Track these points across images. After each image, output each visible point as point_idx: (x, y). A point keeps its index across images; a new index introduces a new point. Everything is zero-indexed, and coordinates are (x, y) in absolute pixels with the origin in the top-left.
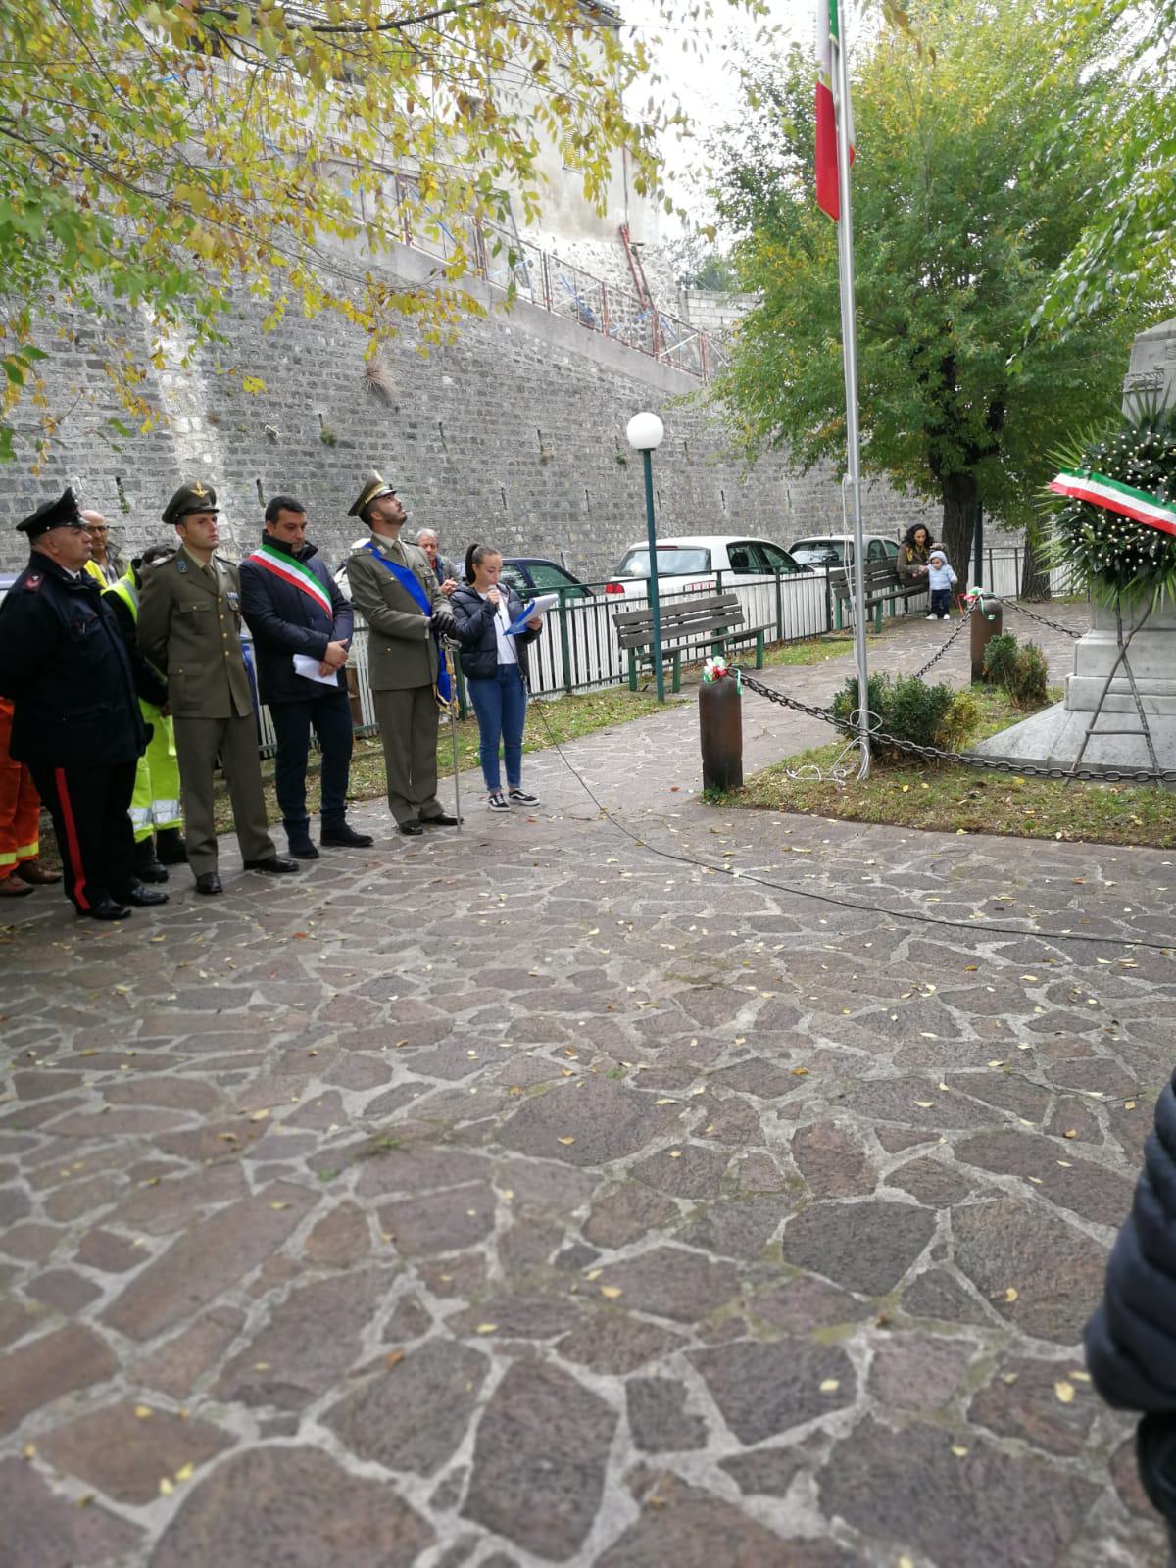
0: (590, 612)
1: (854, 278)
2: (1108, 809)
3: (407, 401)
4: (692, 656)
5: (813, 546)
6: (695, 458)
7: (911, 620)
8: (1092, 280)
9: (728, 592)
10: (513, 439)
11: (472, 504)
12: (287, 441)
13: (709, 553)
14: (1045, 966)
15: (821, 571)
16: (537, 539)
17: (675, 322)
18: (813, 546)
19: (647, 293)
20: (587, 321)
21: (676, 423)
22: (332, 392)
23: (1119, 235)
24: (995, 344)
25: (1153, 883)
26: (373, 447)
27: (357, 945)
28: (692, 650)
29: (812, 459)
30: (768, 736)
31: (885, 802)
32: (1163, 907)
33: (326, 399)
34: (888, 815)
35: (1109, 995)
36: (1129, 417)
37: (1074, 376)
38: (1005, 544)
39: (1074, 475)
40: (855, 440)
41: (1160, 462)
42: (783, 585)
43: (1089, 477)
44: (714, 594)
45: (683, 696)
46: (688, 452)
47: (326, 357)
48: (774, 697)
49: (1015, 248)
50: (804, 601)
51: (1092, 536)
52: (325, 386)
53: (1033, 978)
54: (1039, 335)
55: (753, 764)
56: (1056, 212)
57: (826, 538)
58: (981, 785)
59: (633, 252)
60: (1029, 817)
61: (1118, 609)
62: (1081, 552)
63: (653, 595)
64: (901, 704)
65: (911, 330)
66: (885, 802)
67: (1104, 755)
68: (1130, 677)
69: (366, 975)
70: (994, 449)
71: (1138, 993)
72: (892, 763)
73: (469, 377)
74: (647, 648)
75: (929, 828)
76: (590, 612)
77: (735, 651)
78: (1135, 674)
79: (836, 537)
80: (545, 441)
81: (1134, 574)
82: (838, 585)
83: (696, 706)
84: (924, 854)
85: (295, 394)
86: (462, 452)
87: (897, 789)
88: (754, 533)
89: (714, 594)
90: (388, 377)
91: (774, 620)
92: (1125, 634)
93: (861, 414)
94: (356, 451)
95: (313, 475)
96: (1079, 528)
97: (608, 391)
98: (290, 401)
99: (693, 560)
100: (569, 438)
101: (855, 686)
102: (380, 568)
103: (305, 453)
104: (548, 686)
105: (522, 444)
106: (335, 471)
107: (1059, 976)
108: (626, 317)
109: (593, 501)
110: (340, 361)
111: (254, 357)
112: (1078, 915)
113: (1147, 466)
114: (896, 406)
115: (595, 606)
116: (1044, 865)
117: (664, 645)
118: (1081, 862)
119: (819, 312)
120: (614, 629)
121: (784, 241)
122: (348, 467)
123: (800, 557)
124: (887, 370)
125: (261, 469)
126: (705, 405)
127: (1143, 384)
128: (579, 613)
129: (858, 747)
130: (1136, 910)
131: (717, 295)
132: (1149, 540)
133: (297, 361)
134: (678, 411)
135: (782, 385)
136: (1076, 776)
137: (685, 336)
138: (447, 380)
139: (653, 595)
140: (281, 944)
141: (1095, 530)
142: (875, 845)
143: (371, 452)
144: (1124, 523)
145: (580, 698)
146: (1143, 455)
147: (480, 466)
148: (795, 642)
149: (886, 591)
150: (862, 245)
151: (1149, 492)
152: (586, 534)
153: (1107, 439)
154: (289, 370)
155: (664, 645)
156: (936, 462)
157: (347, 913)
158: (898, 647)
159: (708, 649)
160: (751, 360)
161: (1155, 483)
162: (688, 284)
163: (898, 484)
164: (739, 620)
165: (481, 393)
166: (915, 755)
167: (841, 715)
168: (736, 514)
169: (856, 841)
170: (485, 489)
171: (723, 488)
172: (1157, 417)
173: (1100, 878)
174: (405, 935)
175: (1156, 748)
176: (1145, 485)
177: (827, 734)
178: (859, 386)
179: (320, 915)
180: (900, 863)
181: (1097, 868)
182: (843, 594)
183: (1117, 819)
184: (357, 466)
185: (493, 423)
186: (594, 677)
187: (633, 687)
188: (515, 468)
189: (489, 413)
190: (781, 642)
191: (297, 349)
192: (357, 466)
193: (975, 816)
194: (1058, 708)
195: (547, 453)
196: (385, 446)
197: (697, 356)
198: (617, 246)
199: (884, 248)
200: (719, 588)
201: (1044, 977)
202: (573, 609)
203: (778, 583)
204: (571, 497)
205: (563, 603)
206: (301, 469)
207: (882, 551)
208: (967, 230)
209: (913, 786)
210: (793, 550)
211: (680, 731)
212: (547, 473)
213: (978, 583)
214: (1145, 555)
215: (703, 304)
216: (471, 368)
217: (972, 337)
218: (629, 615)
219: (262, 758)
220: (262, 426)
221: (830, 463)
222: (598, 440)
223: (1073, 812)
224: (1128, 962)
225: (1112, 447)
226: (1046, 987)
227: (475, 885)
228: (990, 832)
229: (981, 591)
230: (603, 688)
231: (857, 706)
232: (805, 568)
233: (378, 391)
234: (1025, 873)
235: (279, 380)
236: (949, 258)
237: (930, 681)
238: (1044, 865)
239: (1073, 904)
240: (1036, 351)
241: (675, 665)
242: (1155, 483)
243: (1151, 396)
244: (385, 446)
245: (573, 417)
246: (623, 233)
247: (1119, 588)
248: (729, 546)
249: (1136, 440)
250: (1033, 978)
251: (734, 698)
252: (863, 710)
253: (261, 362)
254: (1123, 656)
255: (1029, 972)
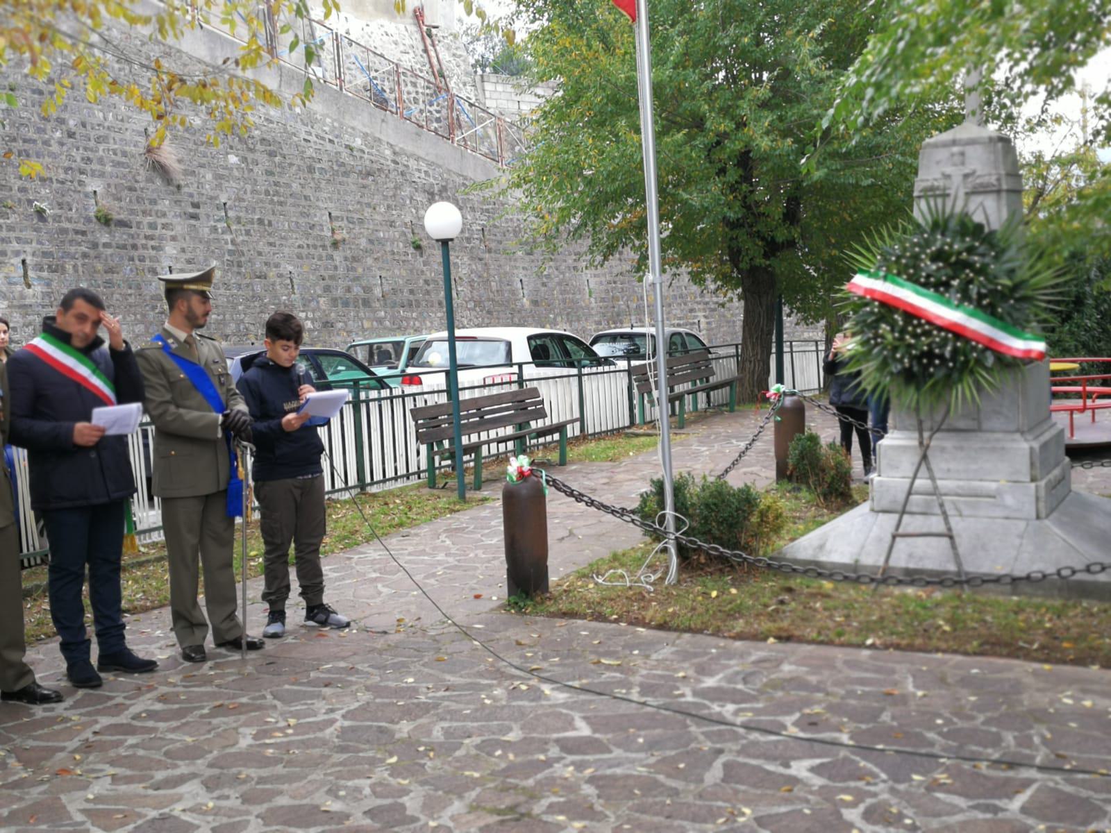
0: (386, 405)
1: (650, 71)
2: (916, 615)
3: (191, 179)
4: (494, 451)
5: (614, 338)
6: (493, 245)
7: (715, 414)
8: (878, 86)
9: (529, 385)
10: (302, 221)
11: (258, 289)
12: (57, 218)
13: (509, 345)
14: (861, 784)
15: (622, 364)
16: (328, 325)
17: (471, 105)
18: (614, 338)
19: (443, 76)
20: (381, 102)
21: (473, 209)
22: (108, 169)
23: (901, 45)
24: (789, 141)
25: (963, 692)
26: (153, 226)
27: (129, 780)
28: (493, 446)
29: (610, 250)
30: (577, 539)
31: (694, 609)
32: (972, 718)
33: (102, 175)
34: (696, 622)
35: (926, 815)
36: (921, 220)
37: (865, 174)
38: (806, 335)
39: (871, 276)
40: (655, 232)
41: (951, 265)
42: (585, 378)
43: (885, 278)
44: (515, 387)
45: (485, 493)
46: (484, 238)
47: (102, 132)
48: (579, 497)
49: (805, 52)
50: (606, 396)
51: (889, 337)
52: (101, 161)
53: (848, 798)
54: (833, 133)
55: (560, 566)
56: (843, 17)
57: (628, 330)
58: (789, 590)
59: (428, 34)
60: (839, 624)
61: (917, 410)
62: (880, 352)
63: (452, 388)
64: (707, 506)
65: (708, 124)
66: (694, 609)
67: (910, 556)
68: (932, 478)
69: (140, 816)
70: (791, 244)
71: (954, 810)
72: (701, 567)
73: (257, 156)
74: (446, 443)
75: (740, 637)
76: (386, 405)
77: (537, 446)
78: (937, 475)
79: (636, 330)
80: (336, 224)
81: (931, 375)
82: (639, 379)
83: (499, 504)
84: (735, 665)
85: (67, 170)
86: (248, 233)
87: (706, 595)
88: (554, 324)
89: (515, 387)
90: (169, 154)
91: (577, 415)
92: (926, 435)
93: (660, 205)
94: (133, 231)
95: (85, 255)
96: (877, 328)
97: (403, 174)
98: (62, 176)
99: (494, 353)
100: (361, 221)
101: (660, 486)
102: (170, 364)
103: (77, 232)
104: (339, 484)
105: (312, 227)
106: (109, 251)
107: (875, 795)
108: (421, 98)
109: (387, 288)
110: (118, 136)
111: (23, 130)
112: (892, 728)
113: (939, 269)
114: (694, 198)
115: (391, 398)
116: (856, 674)
117: (465, 440)
118: (893, 672)
119: (617, 103)
120: (411, 423)
121: (580, 32)
122: (124, 247)
123: (601, 350)
124: (685, 163)
125: (28, 248)
126: (503, 192)
127: (932, 189)
128: (374, 407)
129: (665, 550)
130: (948, 722)
131: (514, 80)
132: (944, 342)
133: (71, 135)
134: (475, 196)
135: (580, 175)
136: (885, 581)
137: (482, 120)
138: (233, 159)
139: (452, 388)
140: (42, 782)
141: (893, 331)
142: (685, 656)
143: (149, 232)
144: (920, 325)
145: (374, 495)
146: (935, 258)
147: (267, 249)
148: (598, 436)
149: (687, 386)
150: (657, 39)
151: (942, 294)
152: (380, 321)
153: (901, 242)
154: (62, 144)
155: (465, 440)
156: (735, 255)
157: (118, 744)
158: (701, 443)
159: (510, 445)
160: (549, 148)
161: (947, 285)
162: (483, 66)
163: (697, 278)
164: (541, 414)
165: (269, 173)
166: (723, 559)
167: (647, 514)
168: (535, 303)
169: (666, 652)
170: (272, 273)
171: (522, 278)
172: (947, 221)
173: (911, 688)
174: (183, 768)
175: (961, 550)
176: (938, 286)
177: (632, 537)
178: (659, 178)
179: (87, 747)
180: (711, 674)
181: (908, 678)
182: (645, 389)
183: (925, 625)
184: (134, 247)
185: (281, 203)
186: (390, 473)
187: (432, 484)
188: (305, 251)
189: (277, 193)
190: (584, 437)
191: (71, 123)
192: (134, 247)
193: (785, 624)
194: (864, 508)
195: (338, 237)
196: (165, 226)
197: (494, 140)
198: (413, 28)
199: (678, 44)
200: (521, 381)
201: (860, 796)
202: (367, 402)
203: (580, 376)
204: (364, 283)
205: (356, 396)
206: (73, 249)
207: (684, 344)
208: (759, 29)
209: (722, 592)
210: (594, 342)
211: (482, 532)
212: (338, 256)
213: (780, 379)
214: (941, 357)
215: (500, 88)
216: (259, 147)
217: (767, 133)
218: (426, 409)
219: (23, 568)
220: (30, 202)
221: (630, 255)
222: (392, 224)
223: (882, 619)
224: (943, 778)
225: (905, 249)
226: (862, 807)
227: (259, 708)
228: (801, 640)
229: (783, 388)
230: (400, 484)
231: (664, 509)
232: (607, 361)
233: (160, 169)
234: (837, 683)
235: (51, 155)
236: (743, 54)
237: (735, 481)
238: (856, 674)
239: (886, 717)
240: (829, 149)
241: (477, 460)
242: (947, 285)
243: (940, 201)
244: (165, 226)
245: (366, 200)
246: (418, 15)
247: (918, 389)
248: (530, 338)
249: (928, 243)
250: (848, 798)
251: (539, 498)
252: (669, 512)
253: (31, 134)
254: (925, 457)
255: (846, 791)
